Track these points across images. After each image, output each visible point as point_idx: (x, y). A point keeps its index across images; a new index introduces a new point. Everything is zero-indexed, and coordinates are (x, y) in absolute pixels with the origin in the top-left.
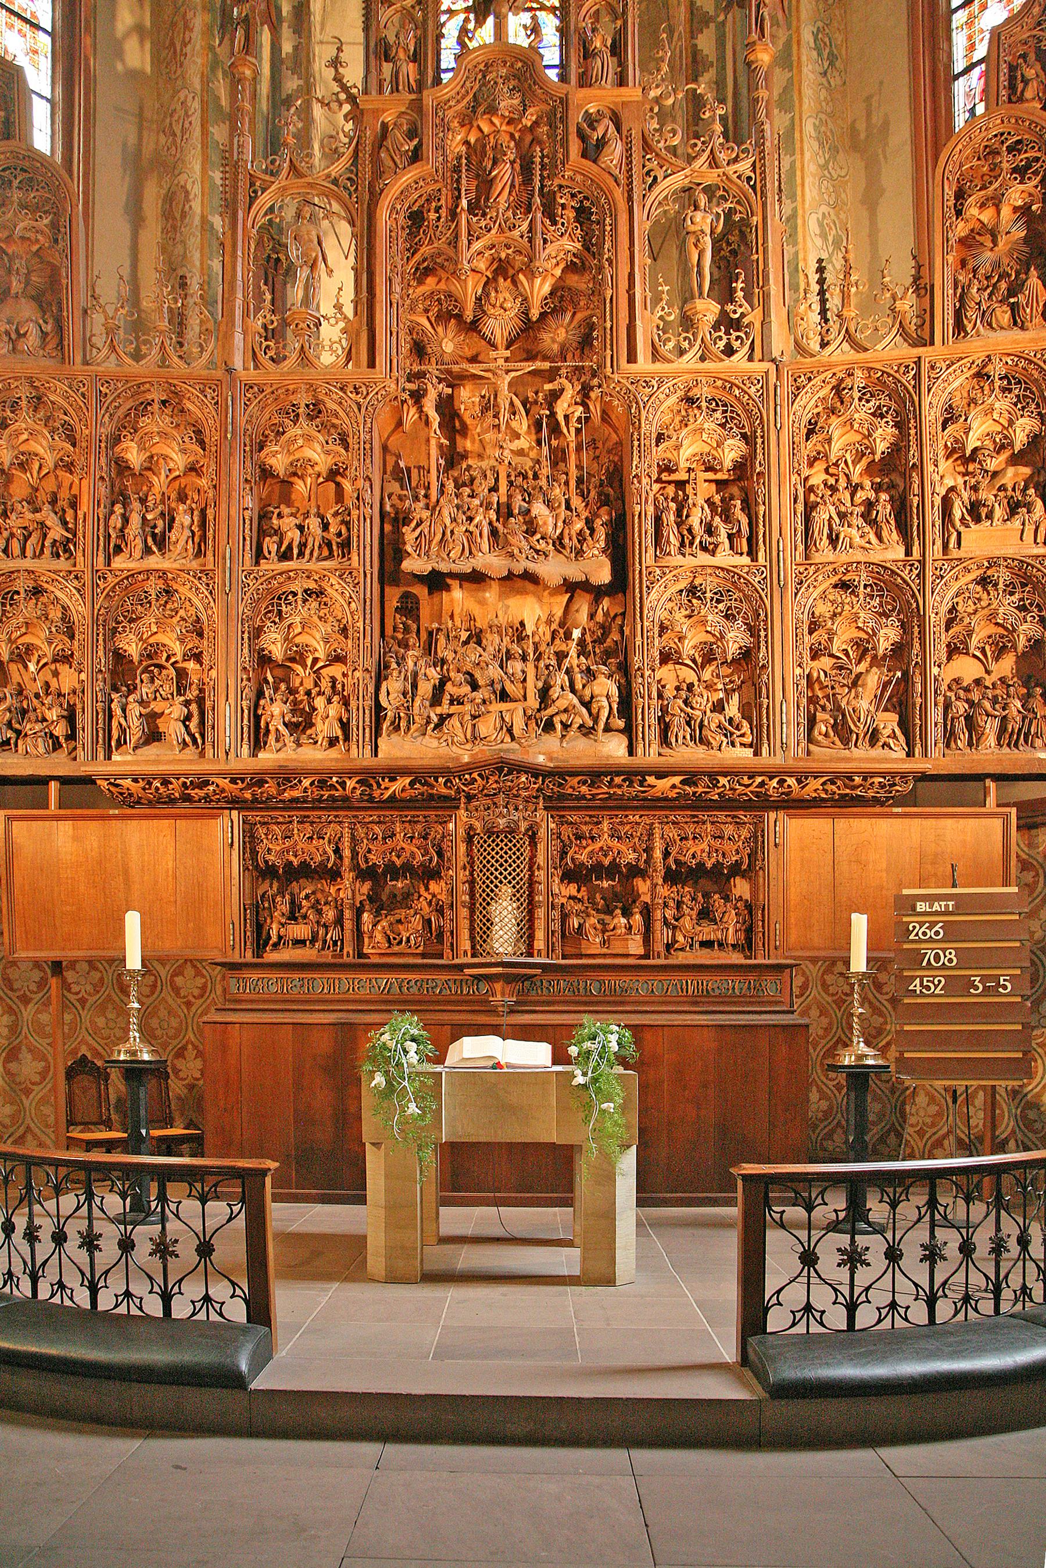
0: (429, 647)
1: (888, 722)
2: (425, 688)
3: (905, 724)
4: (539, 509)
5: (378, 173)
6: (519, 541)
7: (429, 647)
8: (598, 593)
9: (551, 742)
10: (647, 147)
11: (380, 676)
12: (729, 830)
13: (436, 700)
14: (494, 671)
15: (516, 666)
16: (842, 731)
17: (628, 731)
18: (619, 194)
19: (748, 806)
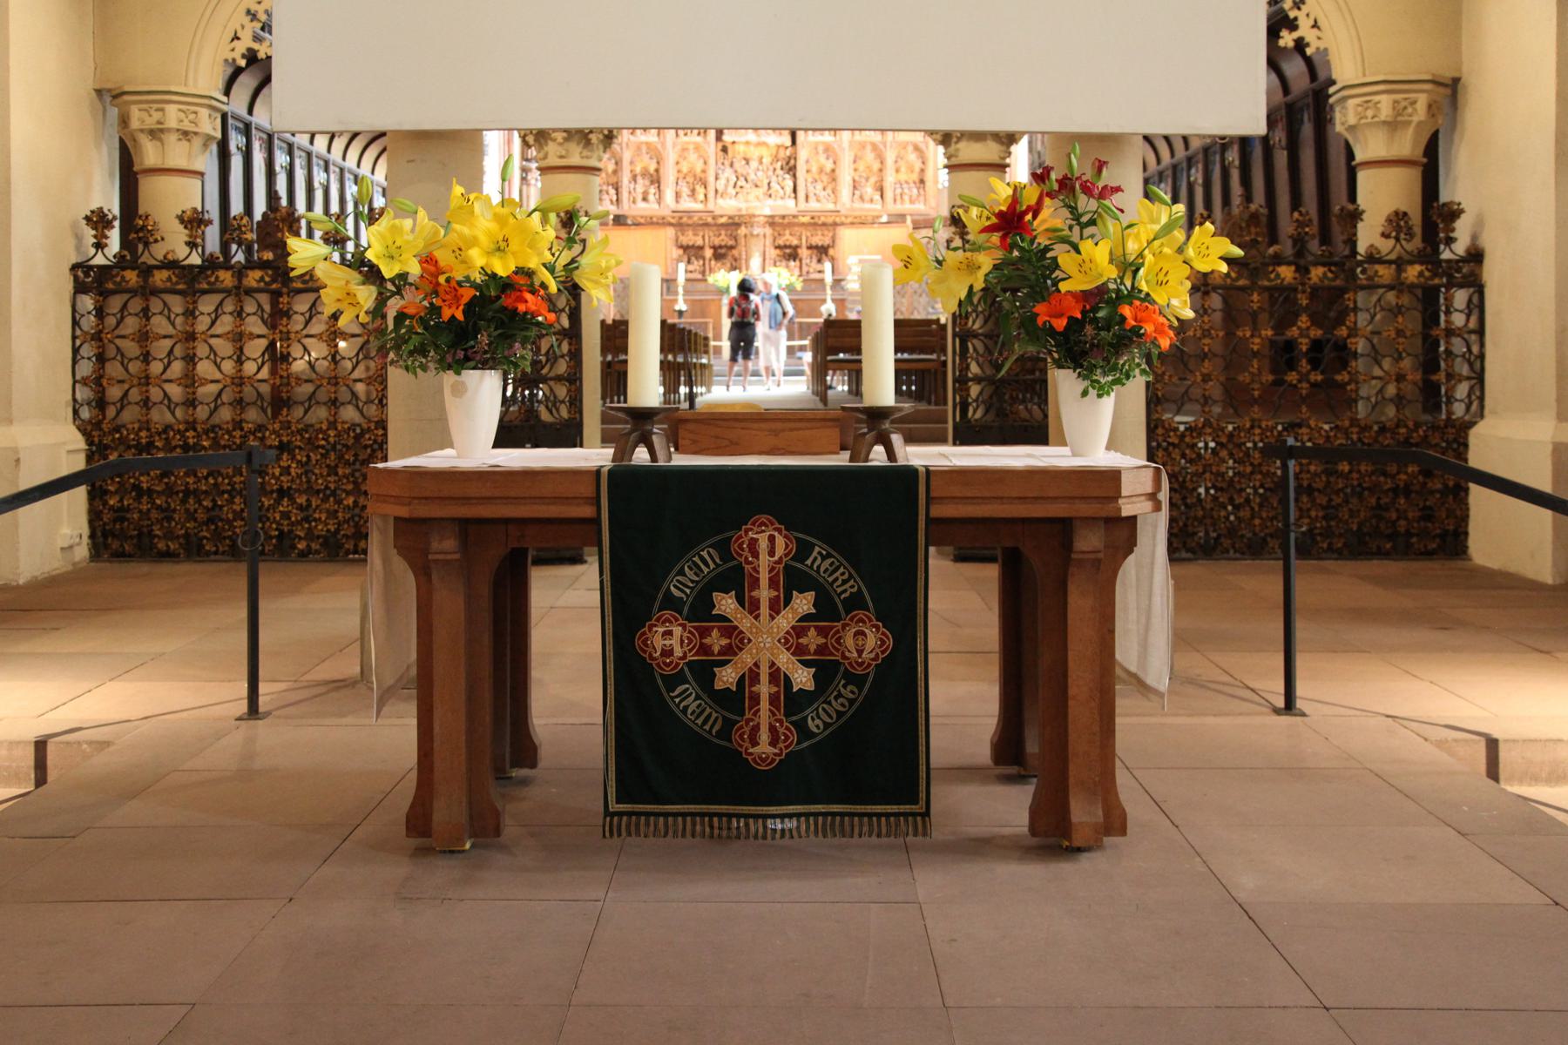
0: (732, 165)
1: (877, 197)
3: (882, 196)
7: (732, 165)
12: (826, 232)
13: (735, 186)
15: (760, 174)
16: (862, 198)
19: (831, 225)
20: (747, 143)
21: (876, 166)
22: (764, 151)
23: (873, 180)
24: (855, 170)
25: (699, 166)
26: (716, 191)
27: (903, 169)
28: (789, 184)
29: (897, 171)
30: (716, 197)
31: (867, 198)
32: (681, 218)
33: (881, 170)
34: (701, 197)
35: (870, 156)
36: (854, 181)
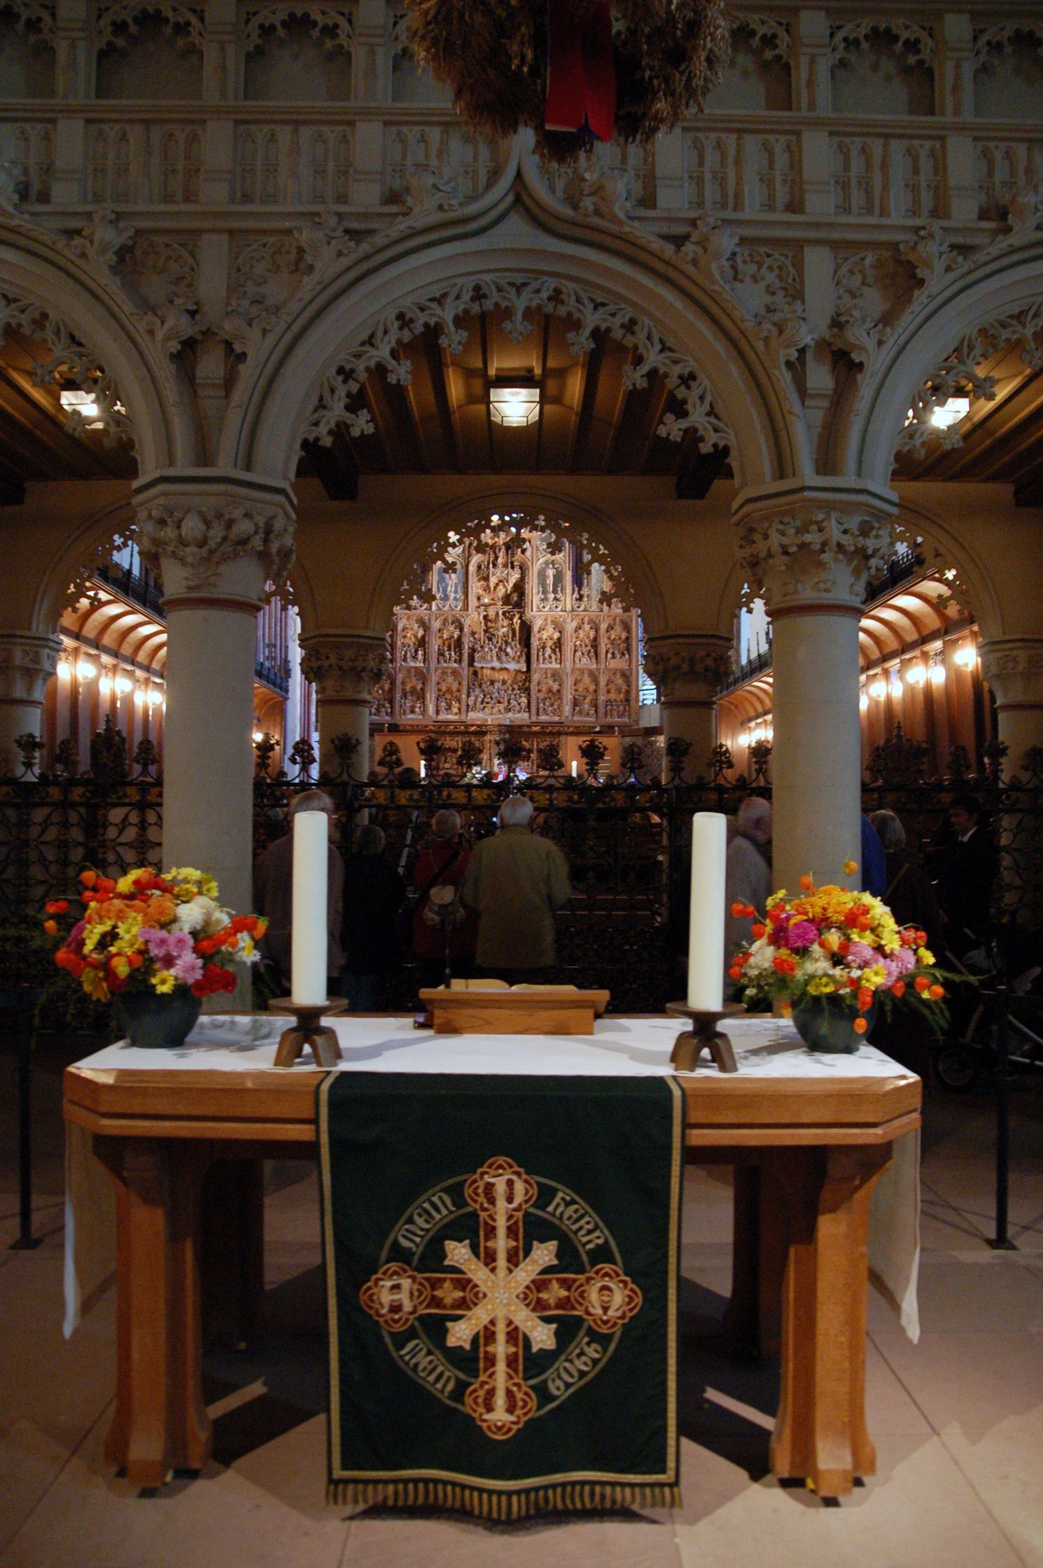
0: (480, 686)
2: (480, 700)
4: (509, 650)
5: (469, 556)
6: (504, 658)
8: (523, 673)
9: (510, 715)
10: (538, 549)
11: (469, 696)
13: (482, 702)
14: (497, 694)
17: (529, 711)
18: (530, 564)
20: (493, 669)
21: (592, 688)
22: (504, 676)
23: (588, 699)
24: (576, 690)
25: (455, 686)
26: (468, 705)
27: (613, 691)
28: (524, 700)
29: (608, 692)
30: (467, 711)
31: (585, 712)
32: (440, 727)
33: (595, 691)
34: (456, 710)
35: (587, 680)
36: (575, 699)
